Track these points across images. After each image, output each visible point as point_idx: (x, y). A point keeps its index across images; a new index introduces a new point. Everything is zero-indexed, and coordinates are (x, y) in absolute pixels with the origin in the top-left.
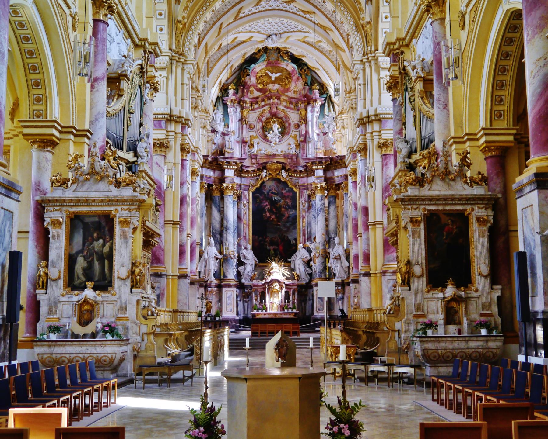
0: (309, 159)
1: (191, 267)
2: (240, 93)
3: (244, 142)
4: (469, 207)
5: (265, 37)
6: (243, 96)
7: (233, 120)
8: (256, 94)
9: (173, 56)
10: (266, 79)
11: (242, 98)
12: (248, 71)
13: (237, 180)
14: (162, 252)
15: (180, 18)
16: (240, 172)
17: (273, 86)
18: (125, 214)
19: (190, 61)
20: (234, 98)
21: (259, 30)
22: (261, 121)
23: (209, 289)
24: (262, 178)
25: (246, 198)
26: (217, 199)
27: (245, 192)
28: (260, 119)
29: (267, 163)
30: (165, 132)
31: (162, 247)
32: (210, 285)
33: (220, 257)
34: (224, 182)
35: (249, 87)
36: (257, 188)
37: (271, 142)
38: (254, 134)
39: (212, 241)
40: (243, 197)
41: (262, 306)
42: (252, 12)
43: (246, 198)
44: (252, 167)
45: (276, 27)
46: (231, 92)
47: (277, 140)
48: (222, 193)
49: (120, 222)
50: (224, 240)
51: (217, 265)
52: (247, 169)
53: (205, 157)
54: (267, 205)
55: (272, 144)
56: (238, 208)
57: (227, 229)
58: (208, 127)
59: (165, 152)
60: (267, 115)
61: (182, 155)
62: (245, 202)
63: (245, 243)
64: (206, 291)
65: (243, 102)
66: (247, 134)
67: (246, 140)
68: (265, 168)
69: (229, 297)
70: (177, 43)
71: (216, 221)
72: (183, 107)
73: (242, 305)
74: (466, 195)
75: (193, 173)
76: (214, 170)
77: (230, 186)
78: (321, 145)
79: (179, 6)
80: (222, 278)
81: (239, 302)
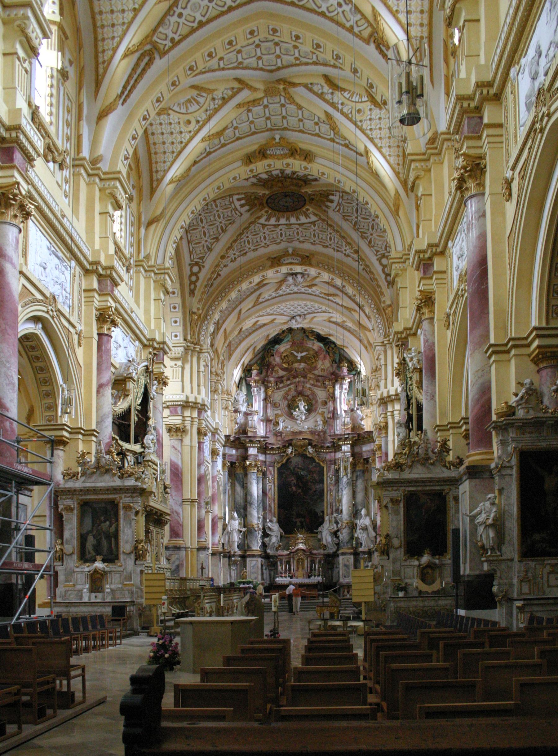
0: (335, 435)
4: (446, 488)
16: (264, 449)
18: (128, 500)
29: (292, 440)
37: (297, 420)
44: (277, 444)
47: (304, 417)
49: (124, 507)
53: (227, 437)
55: (298, 422)
68: (290, 444)
74: (444, 477)
75: (214, 453)
76: (237, 449)
78: (348, 420)
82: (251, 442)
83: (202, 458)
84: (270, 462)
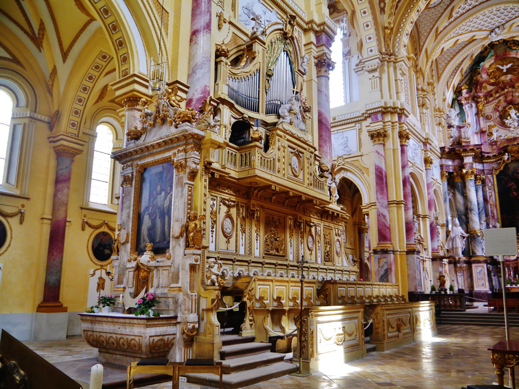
1: (432, 245)
2: (474, 91)
3: (482, 132)
5: (488, 33)
6: (476, 92)
7: (469, 115)
8: (490, 88)
9: (383, 58)
10: (498, 74)
11: (476, 94)
12: (478, 71)
13: (478, 166)
14: (388, 230)
15: (386, 25)
16: (480, 157)
17: (506, 77)
19: (400, 58)
20: (467, 95)
21: (480, 27)
22: (498, 111)
23: (458, 265)
24: (504, 161)
25: (490, 181)
26: (460, 185)
27: (488, 176)
28: (496, 109)
29: (507, 146)
30: (382, 123)
31: (388, 226)
32: (459, 262)
33: (466, 235)
34: (464, 168)
35: (482, 84)
36: (500, 171)
37: (510, 127)
38: (492, 123)
39: (457, 221)
40: (487, 181)
41: (516, 280)
42: (466, 10)
43: (490, 181)
45: (496, 19)
46: (464, 91)
48: (463, 177)
50: (470, 220)
51: (464, 243)
52: (487, 155)
53: (443, 149)
54: (513, 185)
55: (511, 129)
56: (483, 191)
57: (471, 210)
58: (443, 124)
59: (383, 140)
60: (503, 104)
61: (401, 142)
62: (490, 185)
63: (494, 223)
64: (455, 266)
65: (477, 98)
66: (484, 125)
67: (484, 130)
69: (479, 273)
70: (386, 47)
71: (460, 204)
72: (398, 98)
73: (497, 280)
76: (453, 160)
77: (470, 171)
79: (385, 15)
80: (471, 254)
81: (493, 277)
82: (465, 151)
83: (405, 160)
84: (490, 170)
